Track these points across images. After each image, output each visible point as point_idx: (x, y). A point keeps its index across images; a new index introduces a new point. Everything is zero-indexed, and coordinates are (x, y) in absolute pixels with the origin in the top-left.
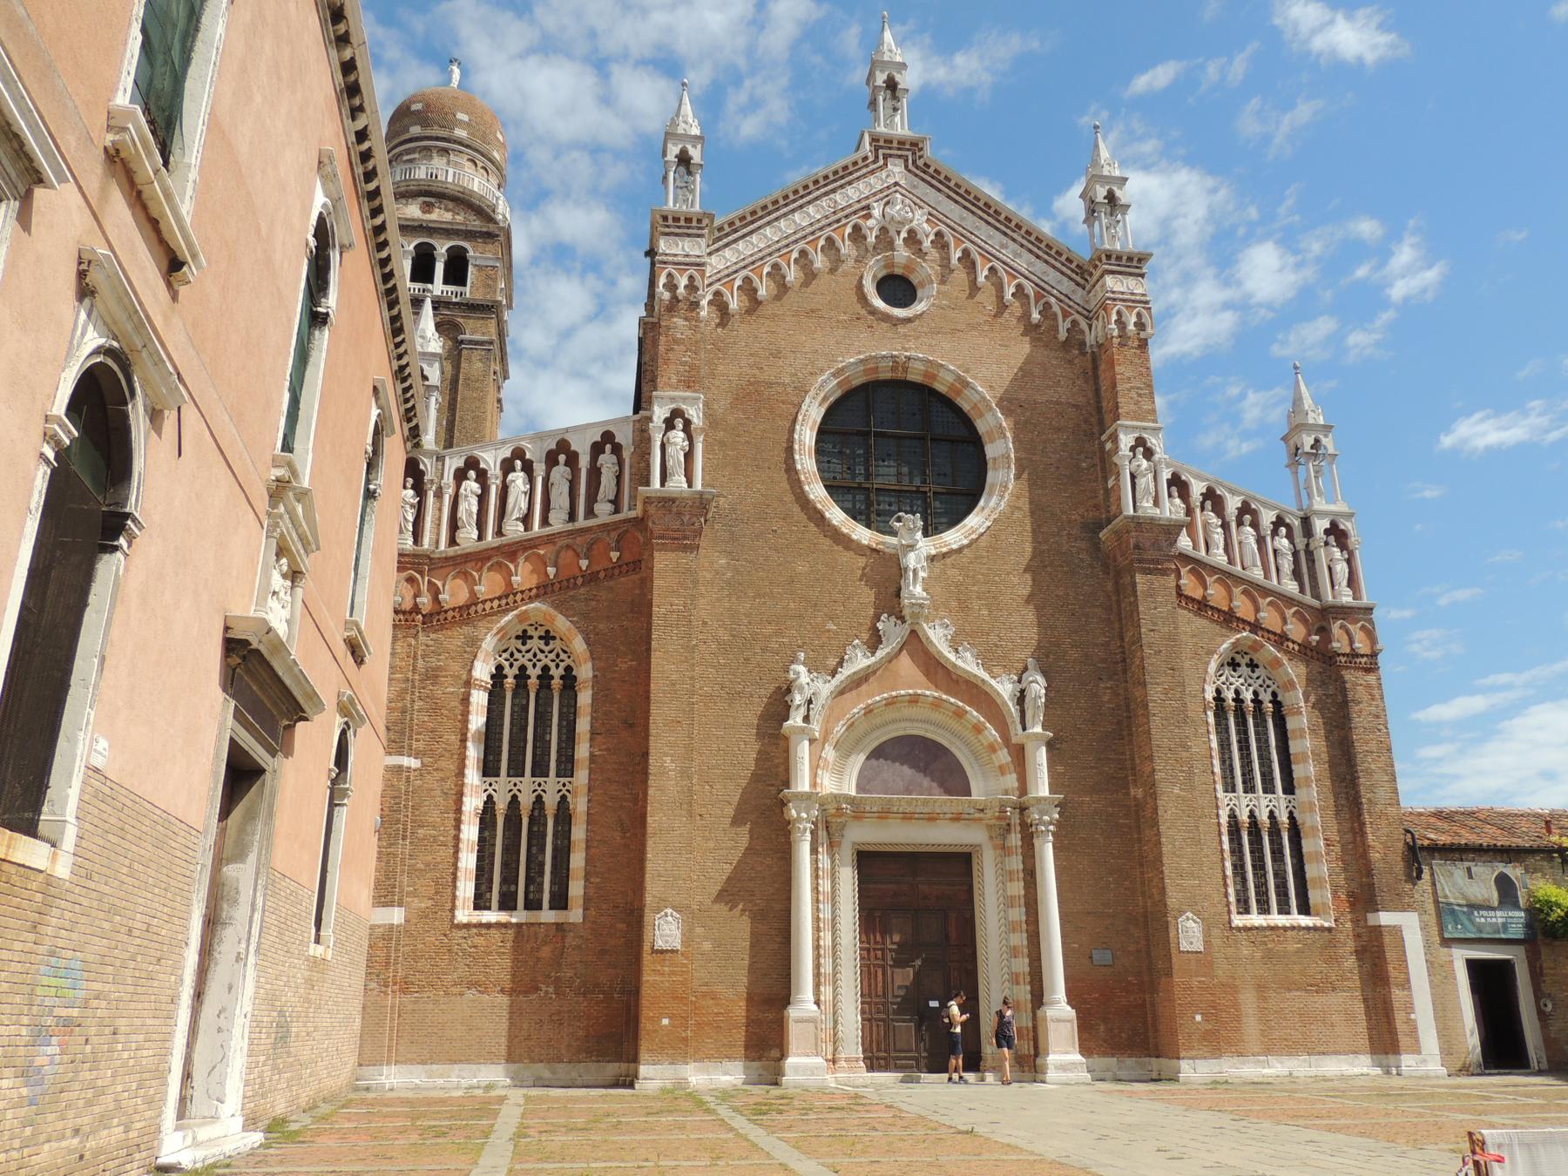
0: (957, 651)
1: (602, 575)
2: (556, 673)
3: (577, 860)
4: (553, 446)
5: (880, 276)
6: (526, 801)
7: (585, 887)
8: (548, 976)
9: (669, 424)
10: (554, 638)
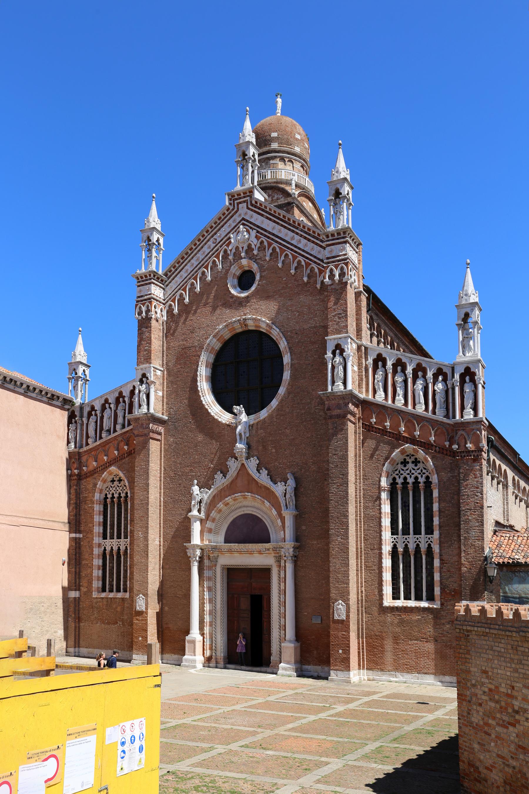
0: (259, 473)
2: (123, 495)
5: (238, 273)
6: (115, 548)
8: (120, 618)
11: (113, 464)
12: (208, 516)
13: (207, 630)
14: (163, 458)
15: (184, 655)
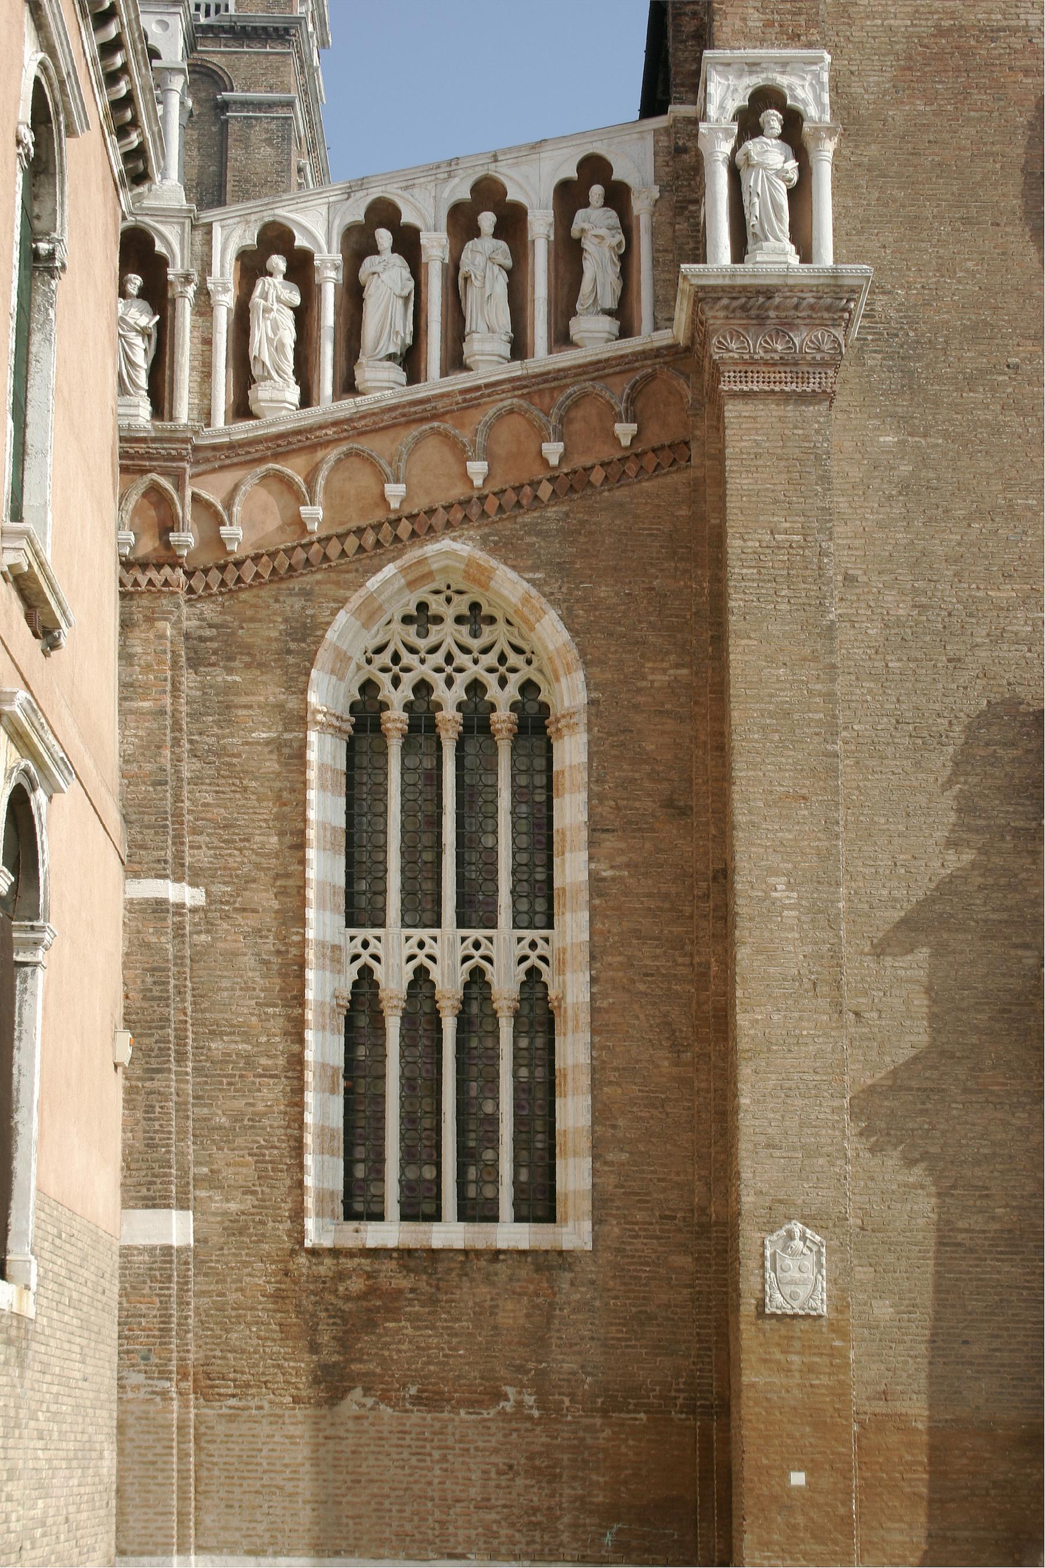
1: (597, 476)
3: (573, 1112)
4: (464, 193)
6: (448, 983)
7: (595, 1172)
9: (749, 124)
10: (491, 620)
11: (449, 525)
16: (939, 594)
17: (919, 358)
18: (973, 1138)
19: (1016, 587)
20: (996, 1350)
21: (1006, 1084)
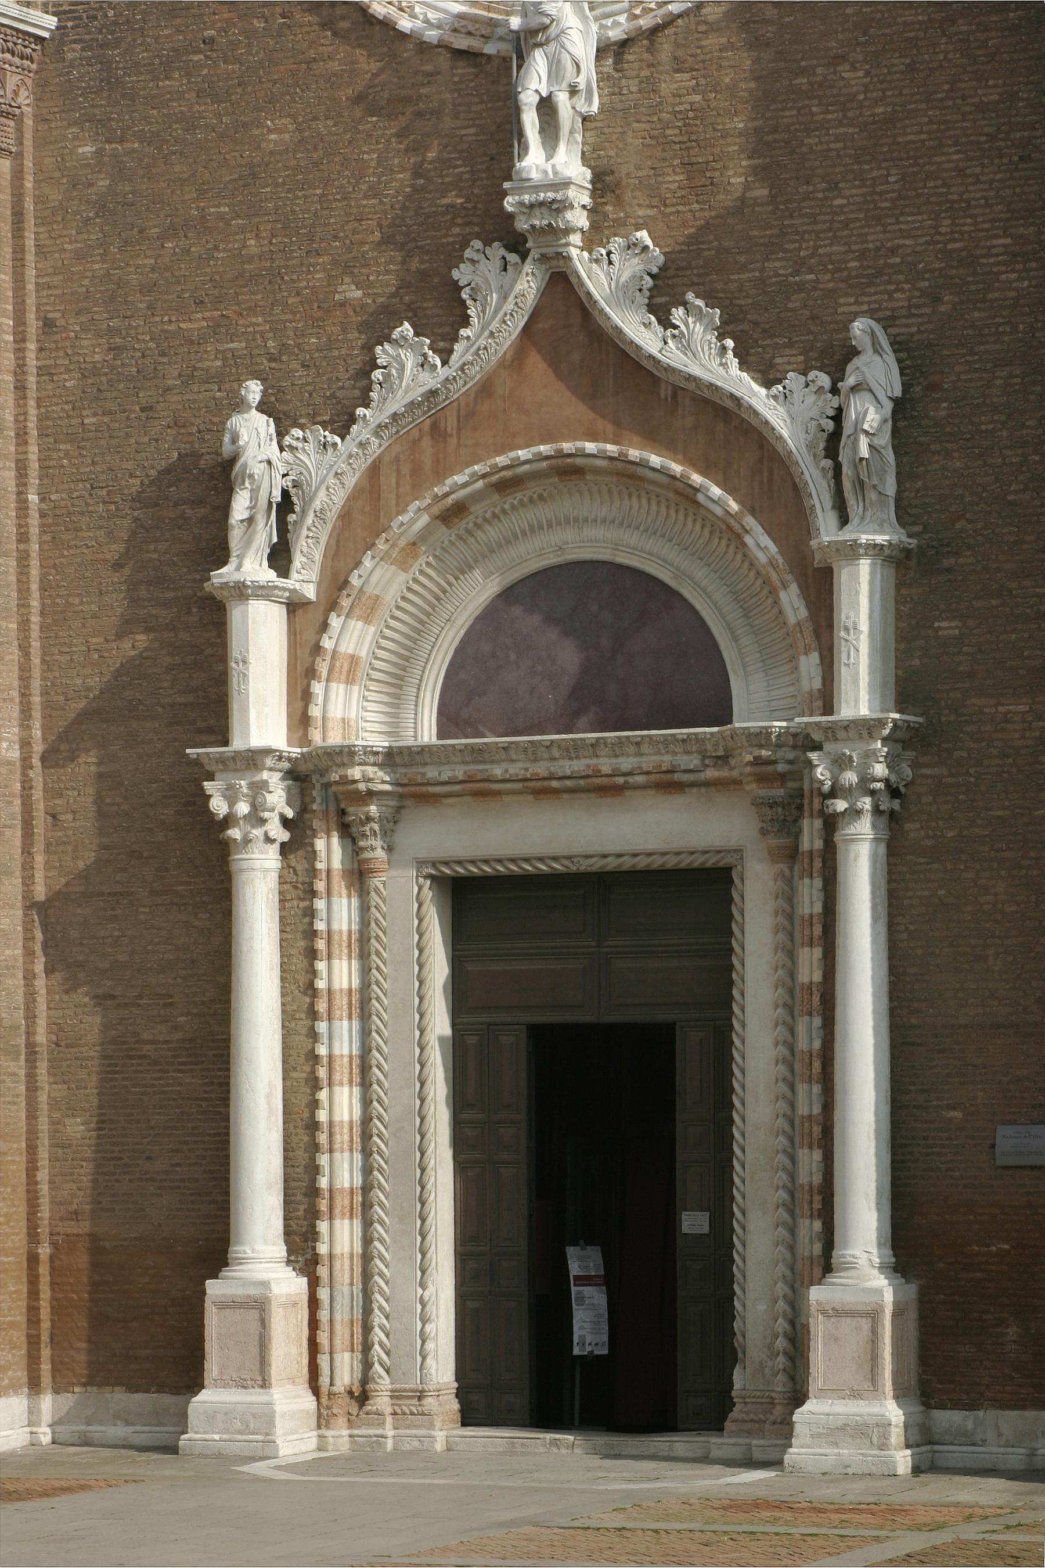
12: (336, 584)
13: (340, 1237)
14: (30, 257)
15: (194, 1383)
16: (132, 332)
17: (117, 43)
18: (159, 943)
19: (208, 314)
20: (178, 1165)
21: (188, 883)
